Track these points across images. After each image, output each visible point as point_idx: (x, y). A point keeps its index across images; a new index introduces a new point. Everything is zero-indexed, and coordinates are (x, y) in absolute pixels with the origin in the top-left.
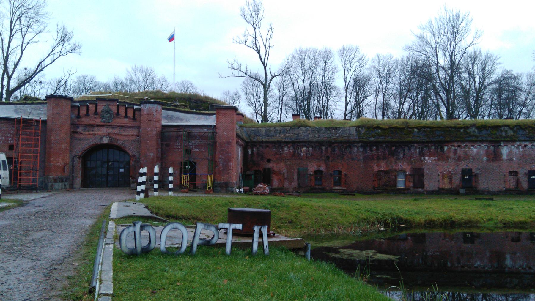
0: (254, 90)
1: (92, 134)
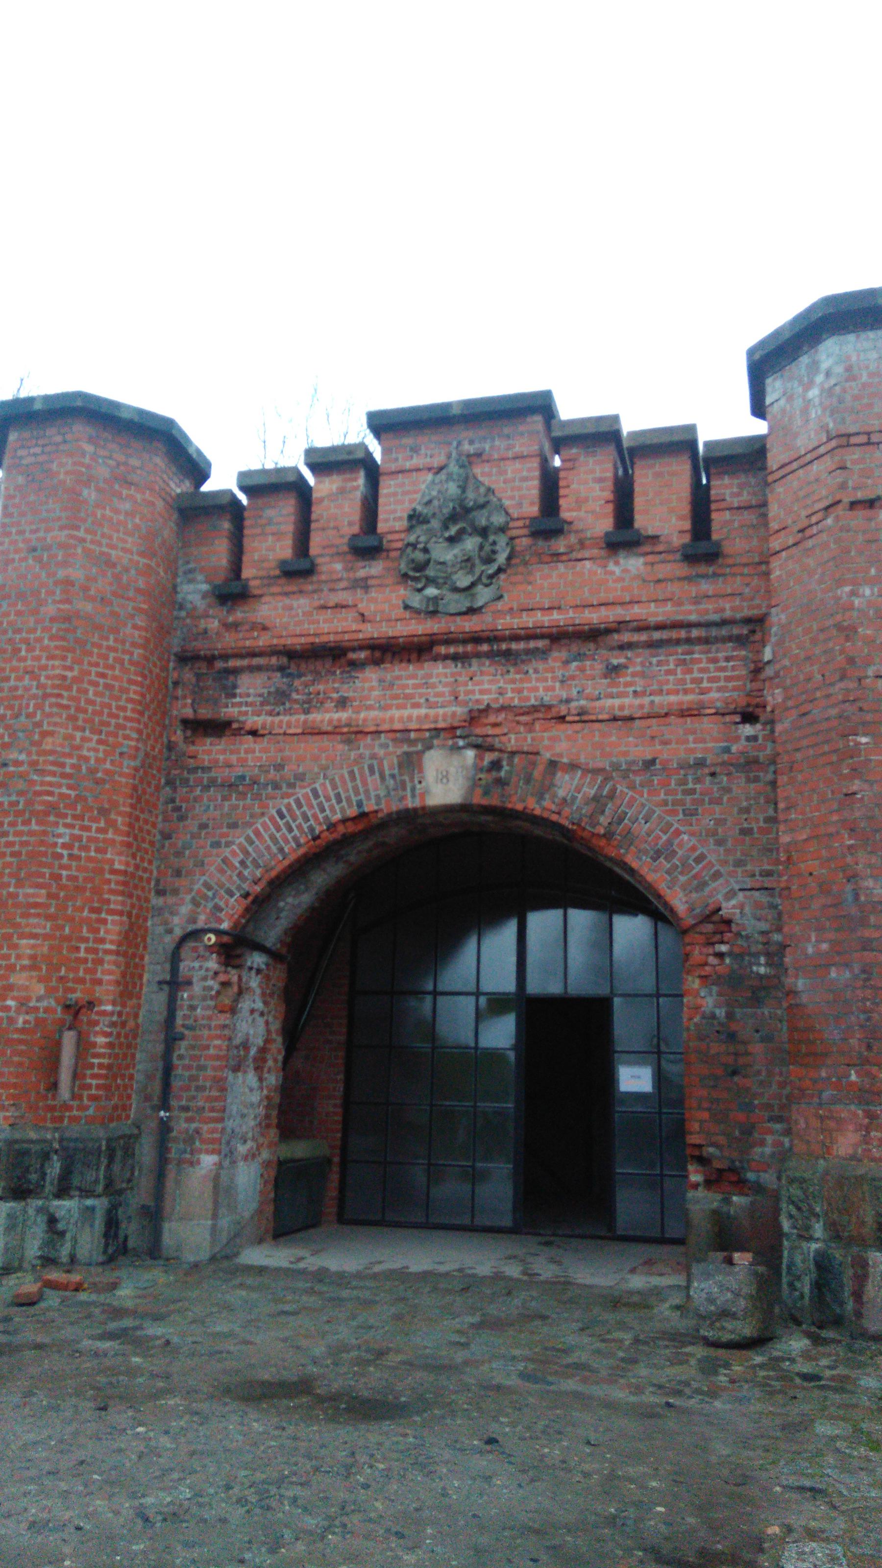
1: (335, 732)
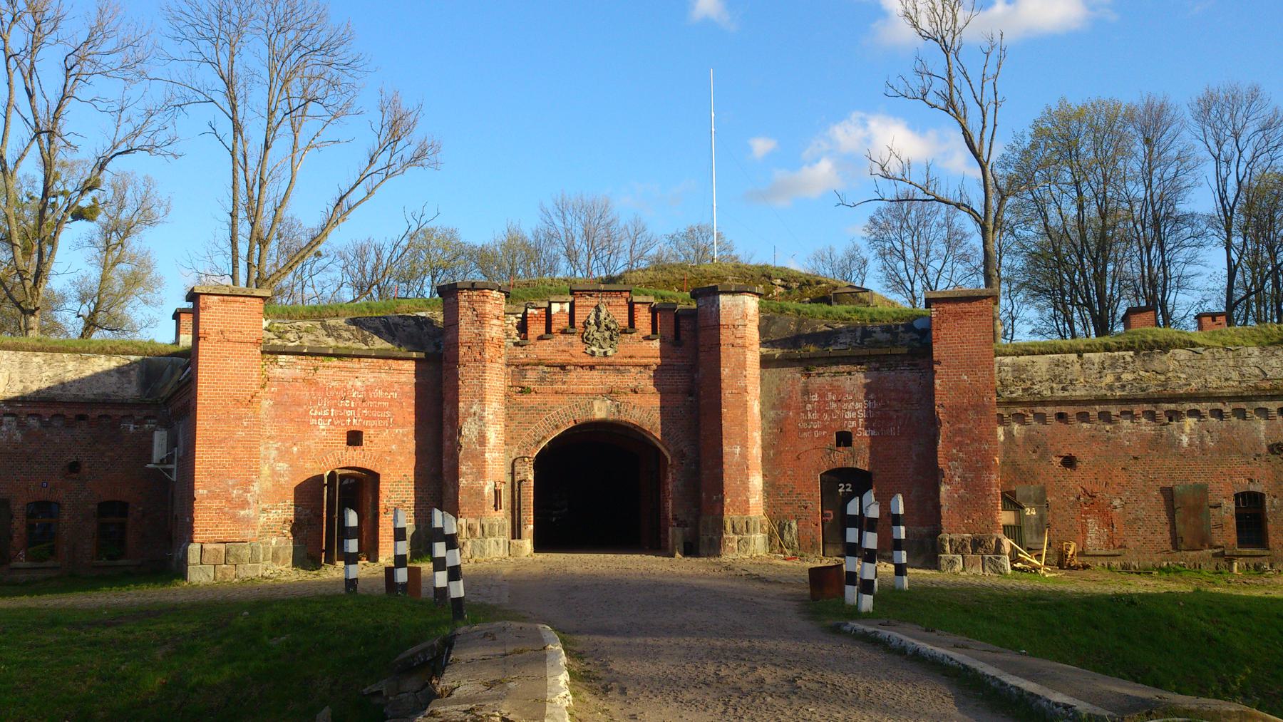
0: (908, 240)
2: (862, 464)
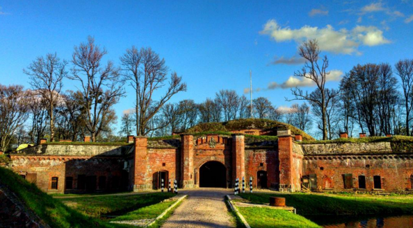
2: (265, 169)
